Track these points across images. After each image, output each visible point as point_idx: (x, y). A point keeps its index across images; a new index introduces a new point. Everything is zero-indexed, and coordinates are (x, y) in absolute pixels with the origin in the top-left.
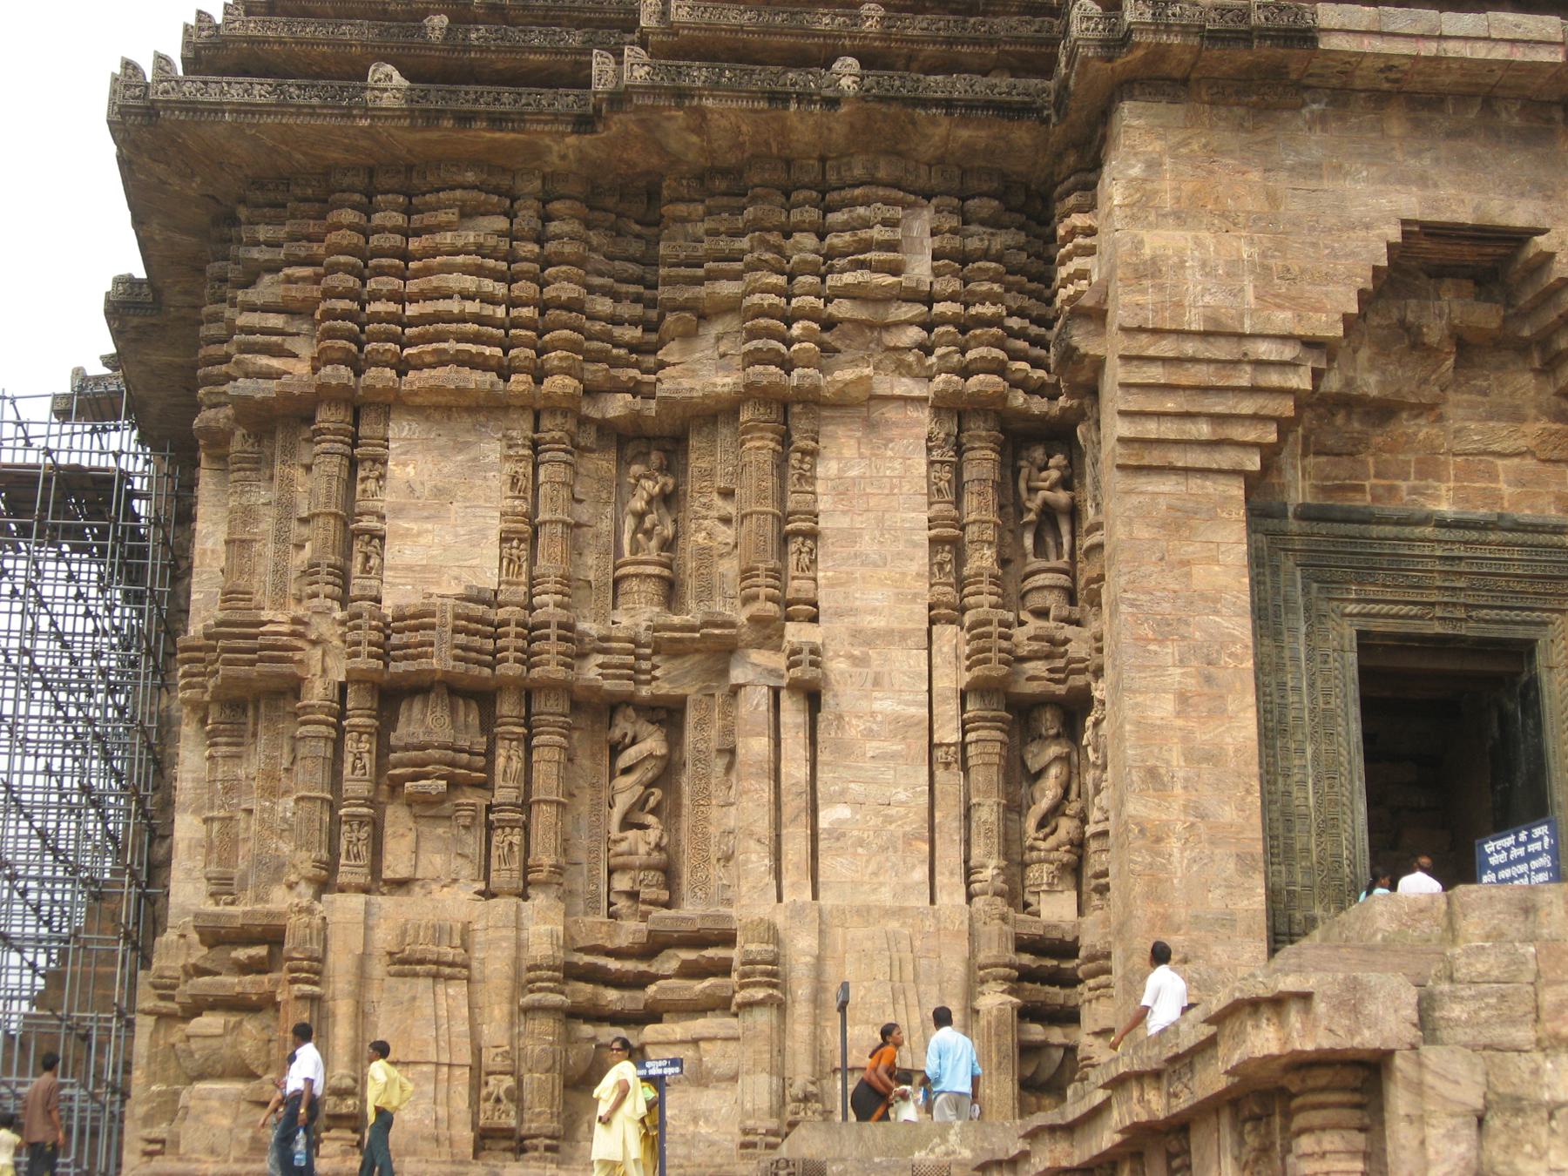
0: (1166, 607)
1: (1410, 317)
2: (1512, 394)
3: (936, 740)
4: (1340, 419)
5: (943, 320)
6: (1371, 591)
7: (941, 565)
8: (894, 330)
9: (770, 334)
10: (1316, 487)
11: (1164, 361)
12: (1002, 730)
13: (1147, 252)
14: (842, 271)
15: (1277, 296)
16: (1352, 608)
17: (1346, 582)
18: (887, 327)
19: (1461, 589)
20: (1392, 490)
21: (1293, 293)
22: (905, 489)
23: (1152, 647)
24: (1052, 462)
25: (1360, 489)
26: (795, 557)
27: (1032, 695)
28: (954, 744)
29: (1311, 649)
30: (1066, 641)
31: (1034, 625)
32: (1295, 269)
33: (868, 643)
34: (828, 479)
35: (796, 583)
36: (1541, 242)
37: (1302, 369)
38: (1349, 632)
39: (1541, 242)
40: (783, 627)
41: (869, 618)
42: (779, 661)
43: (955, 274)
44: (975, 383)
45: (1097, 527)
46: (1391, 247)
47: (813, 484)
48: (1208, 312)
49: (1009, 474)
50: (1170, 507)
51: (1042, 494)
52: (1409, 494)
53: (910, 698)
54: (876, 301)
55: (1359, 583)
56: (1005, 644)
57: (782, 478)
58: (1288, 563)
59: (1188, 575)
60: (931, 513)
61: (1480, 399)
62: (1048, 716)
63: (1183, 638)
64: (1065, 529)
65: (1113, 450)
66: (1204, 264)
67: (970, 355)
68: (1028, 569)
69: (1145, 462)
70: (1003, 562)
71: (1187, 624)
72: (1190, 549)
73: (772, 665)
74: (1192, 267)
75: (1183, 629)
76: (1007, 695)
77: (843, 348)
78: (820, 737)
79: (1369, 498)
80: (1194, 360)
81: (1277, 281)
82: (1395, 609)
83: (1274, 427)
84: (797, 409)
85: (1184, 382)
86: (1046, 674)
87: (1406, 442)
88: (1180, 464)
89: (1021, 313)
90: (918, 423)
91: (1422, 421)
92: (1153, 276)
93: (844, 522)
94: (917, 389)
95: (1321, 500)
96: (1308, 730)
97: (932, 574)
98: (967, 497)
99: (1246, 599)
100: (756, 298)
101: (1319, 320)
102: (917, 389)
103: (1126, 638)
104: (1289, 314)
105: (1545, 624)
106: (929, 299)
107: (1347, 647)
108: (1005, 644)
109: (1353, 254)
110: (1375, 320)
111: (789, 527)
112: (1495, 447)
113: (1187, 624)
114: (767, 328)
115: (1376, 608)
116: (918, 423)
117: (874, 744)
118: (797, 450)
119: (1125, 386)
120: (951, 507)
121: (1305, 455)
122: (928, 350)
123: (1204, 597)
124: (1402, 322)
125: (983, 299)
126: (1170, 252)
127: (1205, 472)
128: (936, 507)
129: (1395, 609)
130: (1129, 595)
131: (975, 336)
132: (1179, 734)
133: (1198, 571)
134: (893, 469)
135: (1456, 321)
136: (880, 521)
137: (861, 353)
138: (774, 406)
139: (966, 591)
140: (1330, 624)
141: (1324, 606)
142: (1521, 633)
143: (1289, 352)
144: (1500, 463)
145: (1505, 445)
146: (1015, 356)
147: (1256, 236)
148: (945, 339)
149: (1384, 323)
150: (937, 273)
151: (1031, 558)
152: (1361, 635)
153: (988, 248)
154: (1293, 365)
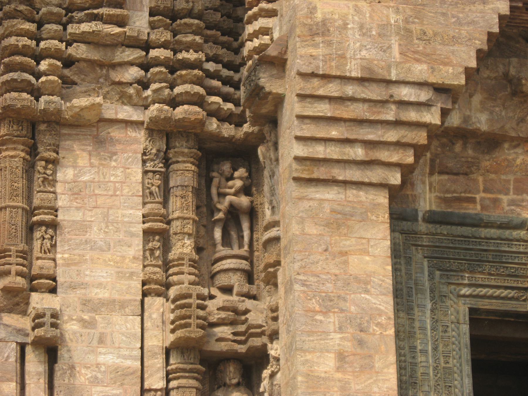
0: (329, 286)
1: (513, 72)
3: (146, 386)
4: (458, 147)
5: (157, 62)
6: (480, 278)
7: (152, 251)
8: (119, 69)
9: (23, 68)
10: (440, 198)
11: (330, 99)
12: (196, 379)
13: (319, 16)
14: (80, 22)
16: (465, 291)
17: (461, 271)
18: (114, 66)
20: (496, 201)
21: (428, 51)
22: (125, 192)
23: (319, 317)
24: (236, 174)
25: (472, 200)
26: (39, 242)
27: (221, 353)
28: (160, 390)
29: (435, 321)
30: (247, 311)
31: (221, 299)
32: (430, 33)
33: (95, 310)
34: (65, 182)
35: (40, 262)
37: (433, 109)
38: (463, 308)
40: (28, 298)
41: (97, 290)
42: (26, 323)
43: (166, 27)
44: (181, 111)
45: (275, 224)
46: (501, 18)
47: (54, 186)
48: (364, 63)
49: (203, 182)
50: (333, 211)
51: (228, 198)
52: (509, 205)
53: (127, 353)
54: (105, 46)
55: (471, 272)
56: (201, 313)
57: (30, 180)
58: (418, 255)
59: (346, 262)
60: (146, 210)
62: (232, 369)
63: (342, 311)
64: (245, 225)
65: (290, 166)
66: (361, 27)
67: (178, 90)
68: (217, 255)
69: (315, 176)
70: (199, 250)
71: (345, 300)
72: (348, 243)
73: (20, 326)
74: (353, 28)
75: (342, 304)
76: (201, 351)
77: (79, 81)
78: (56, 383)
79: (479, 207)
80: (353, 99)
82: (498, 292)
83: (411, 152)
84: (43, 127)
85: (345, 116)
86: (231, 337)
87: (507, 166)
88: (341, 178)
89: (215, 59)
90: (136, 141)
91: (519, 150)
92: (323, 34)
93: (78, 216)
94: (135, 115)
95: (444, 208)
96: (432, 383)
97: (145, 257)
98: (172, 200)
99: (389, 282)
100: (13, 40)
101: (447, 72)
102: (135, 115)
103: (298, 310)
104: (425, 67)
106: (147, 46)
107: (461, 320)
108: (201, 313)
109: (472, 22)
110: (486, 73)
111: (35, 219)
113: (345, 300)
114: (21, 63)
115: (483, 291)
116: (138, 142)
117: (99, 389)
118: (42, 159)
119: (301, 118)
120: (160, 206)
121: (431, 174)
122: (145, 86)
123: (357, 279)
124: (506, 75)
125: (187, 48)
126: (336, 17)
128: (149, 206)
129: (498, 292)
130: (301, 277)
131: (181, 76)
132: (338, 384)
133: (353, 259)
134: (116, 176)
136: (106, 216)
137: (93, 86)
138: (25, 124)
139: (171, 271)
140: (449, 303)
141: (445, 289)
143: (424, 96)
146: (211, 92)
147: (401, 6)
148: (158, 77)
149: (493, 75)
150: (153, 26)
151: (220, 247)
152: (472, 311)
153: (192, 9)
154: (426, 105)
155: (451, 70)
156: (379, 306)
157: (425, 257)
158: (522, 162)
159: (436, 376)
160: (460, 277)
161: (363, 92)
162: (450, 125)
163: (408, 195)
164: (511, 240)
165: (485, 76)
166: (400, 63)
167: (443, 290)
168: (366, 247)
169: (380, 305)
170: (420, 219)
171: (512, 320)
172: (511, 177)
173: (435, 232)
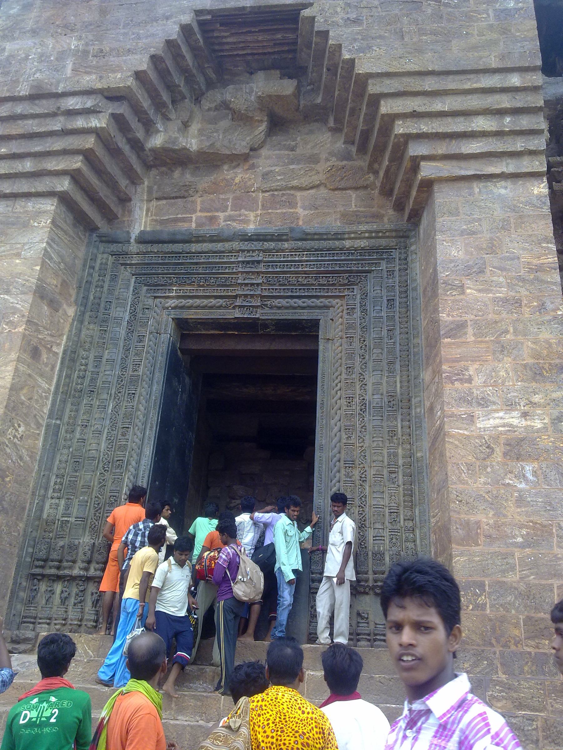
2: (313, 148)
4: (177, 174)
10: (156, 221)
15: (90, 67)
17: (171, 284)
19: (258, 285)
20: (212, 219)
29: (130, 331)
36: (306, 13)
39: (306, 13)
48: (35, 84)
52: (225, 221)
58: (125, 274)
61: (286, 152)
80: (23, 117)
81: (90, 58)
82: (205, 302)
83: (81, 158)
85: (14, 132)
91: (239, 170)
95: (158, 228)
104: (94, 77)
105: (327, 307)
109: (153, 35)
112: (295, 183)
127: (28, 195)
129: (205, 302)
135: (260, 93)
142: (305, 315)
144: (299, 194)
145: (302, 180)
155: (119, 76)
156: (15, 305)
157: (133, 275)
158: (241, 180)
159: (119, 384)
160: (167, 291)
161: (31, 108)
162: (154, 145)
163: (124, 221)
164: (223, 252)
165: (207, 108)
166: (70, 78)
167: (147, 303)
168: (20, 251)
169: (17, 304)
170: (132, 240)
171: (236, 333)
172: (230, 196)
173: (145, 251)
